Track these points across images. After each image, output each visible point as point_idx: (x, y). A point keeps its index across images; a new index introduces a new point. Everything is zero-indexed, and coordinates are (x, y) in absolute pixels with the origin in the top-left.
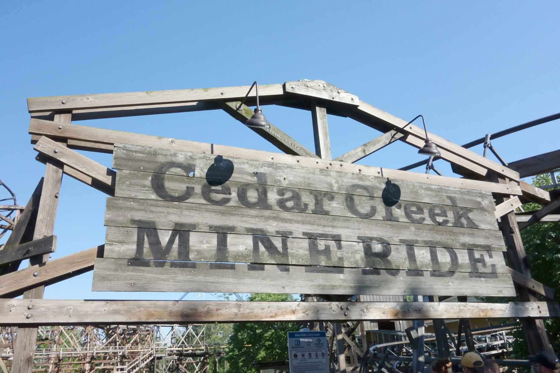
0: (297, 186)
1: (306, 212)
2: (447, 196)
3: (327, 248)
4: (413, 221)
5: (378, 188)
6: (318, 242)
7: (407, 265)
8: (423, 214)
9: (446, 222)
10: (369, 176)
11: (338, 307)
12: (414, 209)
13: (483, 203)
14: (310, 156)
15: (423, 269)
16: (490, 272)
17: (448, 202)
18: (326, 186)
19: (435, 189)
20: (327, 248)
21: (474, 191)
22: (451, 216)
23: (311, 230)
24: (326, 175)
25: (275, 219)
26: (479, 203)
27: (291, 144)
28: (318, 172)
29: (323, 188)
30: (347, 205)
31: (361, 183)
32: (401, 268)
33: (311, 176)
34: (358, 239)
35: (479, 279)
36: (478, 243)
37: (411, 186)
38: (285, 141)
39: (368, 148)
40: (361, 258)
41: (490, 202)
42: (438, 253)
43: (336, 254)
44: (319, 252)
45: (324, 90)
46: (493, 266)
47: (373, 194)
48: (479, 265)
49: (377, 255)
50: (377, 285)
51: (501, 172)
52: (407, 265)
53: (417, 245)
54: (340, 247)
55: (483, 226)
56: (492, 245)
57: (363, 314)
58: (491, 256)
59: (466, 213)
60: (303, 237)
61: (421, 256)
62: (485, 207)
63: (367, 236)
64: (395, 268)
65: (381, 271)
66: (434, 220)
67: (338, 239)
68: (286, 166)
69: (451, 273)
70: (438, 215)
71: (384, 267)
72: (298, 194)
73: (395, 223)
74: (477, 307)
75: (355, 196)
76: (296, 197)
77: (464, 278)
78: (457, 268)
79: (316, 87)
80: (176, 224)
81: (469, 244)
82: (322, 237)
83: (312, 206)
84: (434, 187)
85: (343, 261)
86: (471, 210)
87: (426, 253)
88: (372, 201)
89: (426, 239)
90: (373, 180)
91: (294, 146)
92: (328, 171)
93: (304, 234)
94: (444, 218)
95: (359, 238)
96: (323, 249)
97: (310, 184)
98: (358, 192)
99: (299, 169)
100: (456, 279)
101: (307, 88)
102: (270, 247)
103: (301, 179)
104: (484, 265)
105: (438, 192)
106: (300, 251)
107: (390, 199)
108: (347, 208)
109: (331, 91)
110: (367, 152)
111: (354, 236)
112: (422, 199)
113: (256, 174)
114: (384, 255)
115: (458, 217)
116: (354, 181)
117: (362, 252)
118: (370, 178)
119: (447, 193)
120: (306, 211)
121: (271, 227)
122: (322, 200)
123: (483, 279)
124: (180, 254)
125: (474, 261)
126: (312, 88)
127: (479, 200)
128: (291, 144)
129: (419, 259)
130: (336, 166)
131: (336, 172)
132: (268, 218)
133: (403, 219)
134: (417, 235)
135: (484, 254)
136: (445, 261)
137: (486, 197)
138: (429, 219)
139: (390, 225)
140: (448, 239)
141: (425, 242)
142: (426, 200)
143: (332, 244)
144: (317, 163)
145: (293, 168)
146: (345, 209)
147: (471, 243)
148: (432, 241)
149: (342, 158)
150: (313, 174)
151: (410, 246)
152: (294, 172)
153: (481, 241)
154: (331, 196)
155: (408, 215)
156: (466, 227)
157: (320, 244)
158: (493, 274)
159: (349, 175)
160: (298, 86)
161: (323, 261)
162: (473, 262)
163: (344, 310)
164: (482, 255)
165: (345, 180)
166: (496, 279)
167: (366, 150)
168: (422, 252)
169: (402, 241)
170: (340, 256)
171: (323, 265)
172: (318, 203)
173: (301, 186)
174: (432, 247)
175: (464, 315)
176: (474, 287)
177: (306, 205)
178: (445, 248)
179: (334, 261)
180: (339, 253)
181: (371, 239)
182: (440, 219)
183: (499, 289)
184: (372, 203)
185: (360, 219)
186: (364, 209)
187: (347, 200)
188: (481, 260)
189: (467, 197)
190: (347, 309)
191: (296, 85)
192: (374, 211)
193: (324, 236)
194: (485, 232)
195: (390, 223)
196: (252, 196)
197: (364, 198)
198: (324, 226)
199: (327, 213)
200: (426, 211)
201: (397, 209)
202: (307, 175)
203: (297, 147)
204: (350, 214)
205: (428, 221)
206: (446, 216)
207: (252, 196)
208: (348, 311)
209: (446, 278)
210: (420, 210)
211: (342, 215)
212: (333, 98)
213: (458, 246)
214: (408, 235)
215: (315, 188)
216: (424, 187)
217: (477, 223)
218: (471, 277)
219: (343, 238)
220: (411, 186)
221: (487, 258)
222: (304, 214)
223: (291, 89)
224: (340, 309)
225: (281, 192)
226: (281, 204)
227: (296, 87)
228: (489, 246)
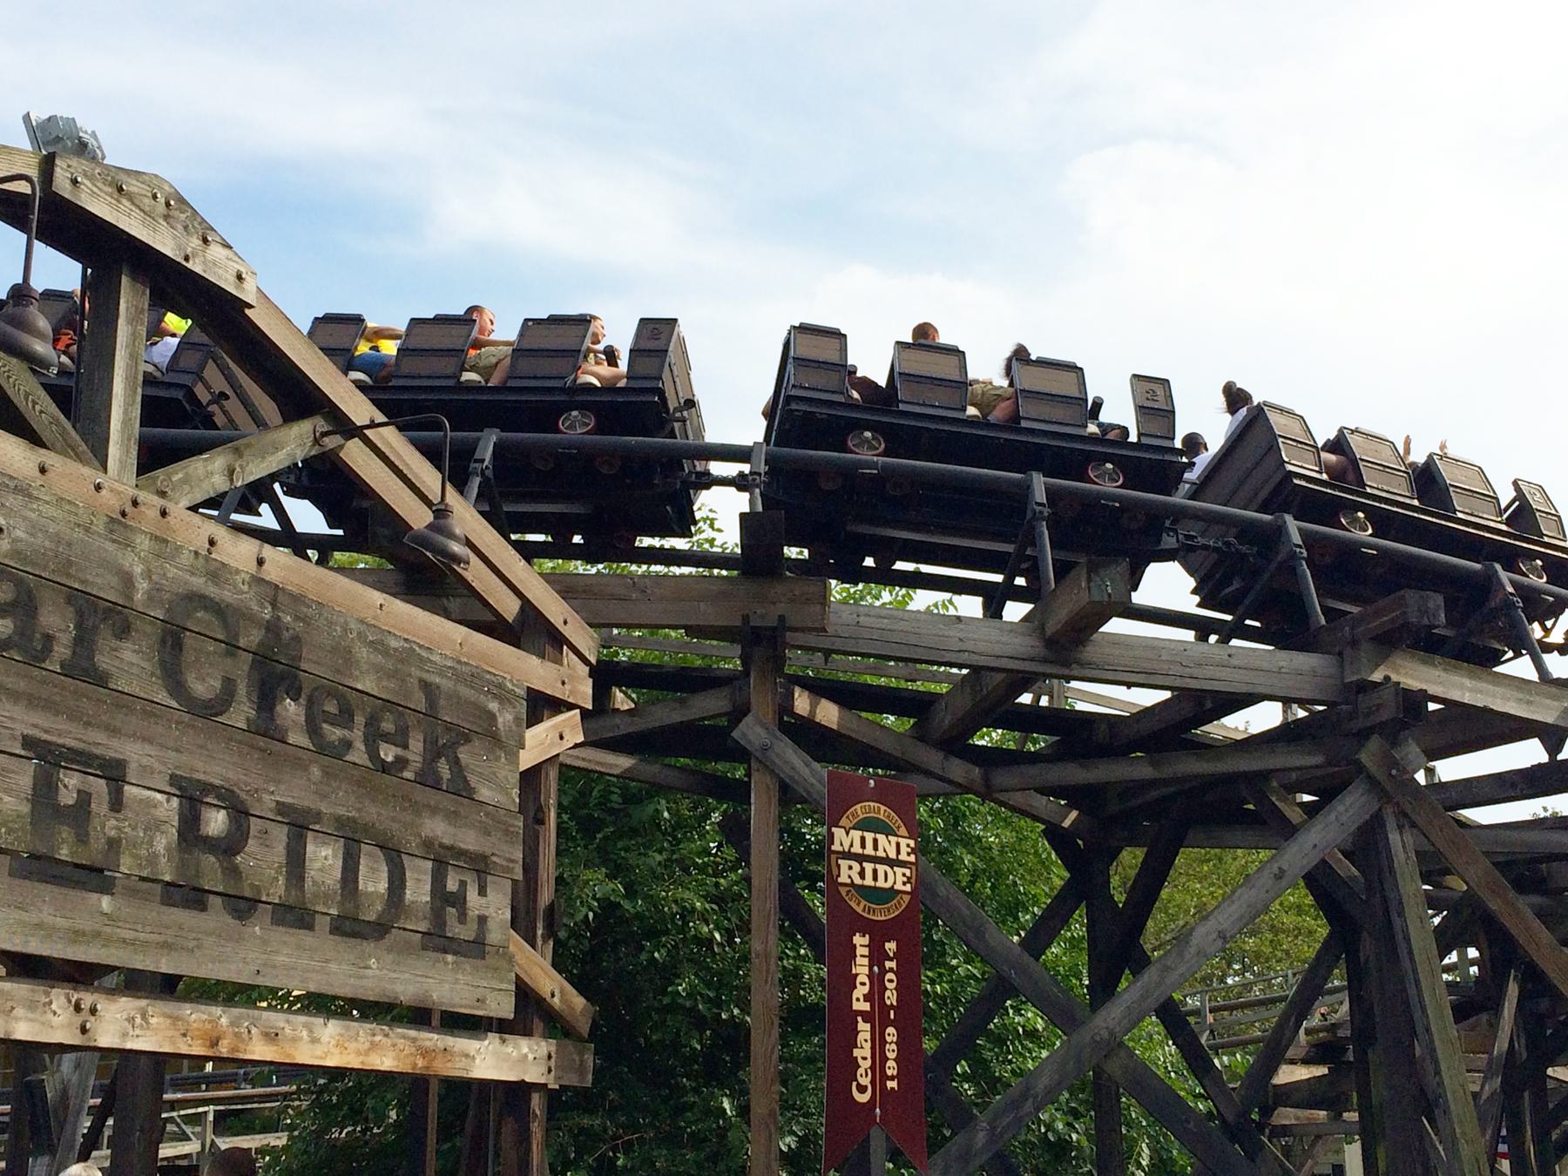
0: (34, 564)
1: (43, 665)
2: (420, 680)
3: (84, 798)
4: (323, 748)
5: (251, 618)
6: (61, 776)
7: (277, 891)
8: (351, 729)
9: (401, 763)
10: (238, 571)
11: (70, 1001)
12: (331, 707)
13: (500, 720)
14: (76, 454)
15: (317, 909)
16: (471, 939)
17: (419, 701)
18: (114, 581)
19: (396, 650)
20: (84, 798)
21: (488, 677)
22: (416, 745)
23: (46, 732)
24: (119, 543)
26: (492, 717)
27: (27, 395)
28: (100, 525)
29: (105, 587)
30: (162, 663)
31: (212, 591)
32: (264, 899)
33: (79, 534)
34: (171, 785)
35: (441, 956)
36: (463, 846)
37: (338, 628)
38: (9, 377)
39: (245, 464)
40: (168, 849)
41: (517, 719)
42: (362, 861)
43: (106, 824)
44: (60, 813)
45: (166, 217)
46: (482, 920)
47: (236, 637)
49: (211, 845)
50: (192, 944)
51: (557, 621)
52: (277, 891)
53: (317, 827)
54: (117, 804)
55: (485, 793)
56: (493, 854)
57: (131, 1033)
58: (482, 892)
59: (454, 745)
60: (23, 753)
61: (317, 865)
62: (503, 734)
63: (197, 776)
64: (248, 894)
65: (211, 897)
66: (373, 754)
67: (115, 773)
68: (12, 484)
69: (379, 930)
70: (387, 738)
71: (220, 889)
72: (29, 592)
74: (414, 1040)
75: (188, 633)
77: (405, 950)
78: (398, 918)
79: (146, 201)
81: (441, 845)
82: (78, 763)
83: (62, 650)
84: (394, 643)
85: (118, 853)
87: (335, 856)
88: (229, 661)
89: (341, 811)
90: (245, 588)
91: (34, 403)
92: (126, 526)
93: (28, 742)
94: (399, 751)
95: (174, 780)
96: (71, 802)
97: (70, 563)
98: (199, 620)
99: (47, 503)
100: (389, 950)
101: (116, 195)
103: (47, 543)
104: (462, 917)
105: (402, 661)
106: (7, 799)
107: (277, 661)
108: (158, 672)
109: (186, 228)
110: (238, 480)
111: (160, 772)
112: (357, 679)
114: (229, 846)
115: (434, 751)
116: (194, 580)
117: (174, 831)
118: (238, 578)
119: (422, 669)
120: (44, 661)
122: (95, 628)
123: (450, 958)
125: (445, 900)
126: (133, 203)
127: (493, 706)
128: (27, 395)
129: (312, 873)
130: (147, 512)
131: (151, 540)
133: (298, 738)
134: (324, 797)
135: (469, 881)
136: (373, 889)
137: (511, 703)
138: (363, 748)
139: (263, 750)
140: (393, 819)
141: (340, 822)
142: (367, 684)
143: (99, 786)
144: (98, 488)
145: (30, 496)
146: (153, 674)
147: (446, 841)
148: (354, 820)
149: (165, 483)
150: (87, 530)
151: (299, 825)
152: (33, 510)
153: (469, 840)
155: (313, 729)
156: (445, 788)
157: (65, 786)
158: (476, 948)
159: (186, 558)
160: (91, 178)
161: (65, 846)
162: (439, 904)
163: (83, 1013)
164: (463, 884)
165: (172, 572)
166: (479, 962)
167: (238, 469)
168: (323, 854)
169: (282, 808)
170: (113, 833)
171: (63, 858)
172: (84, 640)
173: (45, 568)
174: (352, 838)
175: (378, 1062)
176: (423, 980)
177: (49, 639)
178: (381, 847)
179: (93, 853)
180: (113, 822)
181: (208, 788)
182: (388, 753)
183: (479, 993)
185: (187, 717)
186: (203, 686)
187: (163, 642)
188: (458, 900)
189: (465, 692)
190: (93, 1011)
191: (85, 175)
193: (83, 760)
194: (487, 814)
195: (262, 742)
197: (211, 647)
198: (88, 724)
199: (101, 680)
200: (360, 720)
201: (288, 700)
202: (68, 531)
203: (41, 412)
204: (162, 697)
205: (359, 755)
206: (406, 747)
208: (92, 1019)
209: (365, 943)
211: (142, 695)
212: (187, 259)
213: (413, 845)
214: (297, 791)
215: (83, 582)
216: (370, 638)
217: (473, 780)
218: (424, 948)
219: (131, 778)
220: (338, 628)
221: (472, 895)
222: (36, 672)
223: (68, 185)
224: (72, 1009)
227: (86, 182)
228: (484, 858)
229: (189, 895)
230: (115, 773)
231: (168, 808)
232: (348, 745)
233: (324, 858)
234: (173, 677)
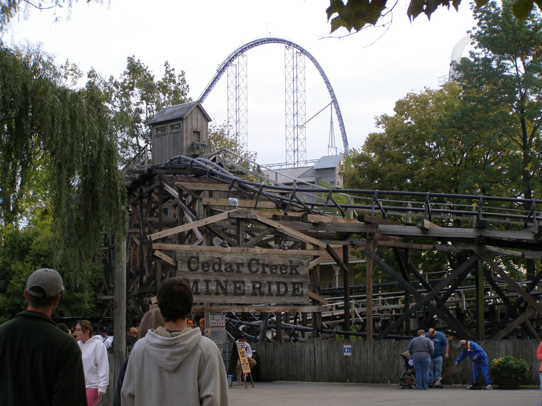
9: (286, 273)
17: (289, 263)
22: (289, 270)
25: (224, 276)
26: (303, 262)
29: (240, 262)
46: (302, 291)
48: (296, 291)
54: (244, 286)
55: (301, 273)
66: (281, 271)
70: (284, 269)
73: (265, 275)
76: (231, 266)
80: (195, 280)
83: (236, 270)
86: (298, 266)
89: (277, 281)
93: (233, 281)
102: (222, 287)
104: (299, 291)
113: (218, 258)
115: (292, 270)
121: (222, 279)
124: (196, 290)
125: (294, 289)
127: (303, 261)
132: (221, 275)
141: (276, 282)
154: (242, 265)
155: (271, 271)
158: (302, 295)
164: (298, 287)
169: (267, 282)
172: (238, 268)
174: (278, 283)
182: (284, 271)
184: (258, 266)
186: (254, 269)
188: (298, 289)
192: (258, 270)
195: (263, 274)
196: (217, 268)
199: (241, 272)
200: (279, 268)
205: (279, 272)
207: (217, 268)
210: (276, 268)
214: (270, 279)
217: (299, 272)
221: (300, 289)
225: (226, 265)
226: (226, 269)
229: (254, 294)
230: (243, 282)
231: (250, 285)
232: (277, 272)
233: (274, 288)
234: (250, 270)
